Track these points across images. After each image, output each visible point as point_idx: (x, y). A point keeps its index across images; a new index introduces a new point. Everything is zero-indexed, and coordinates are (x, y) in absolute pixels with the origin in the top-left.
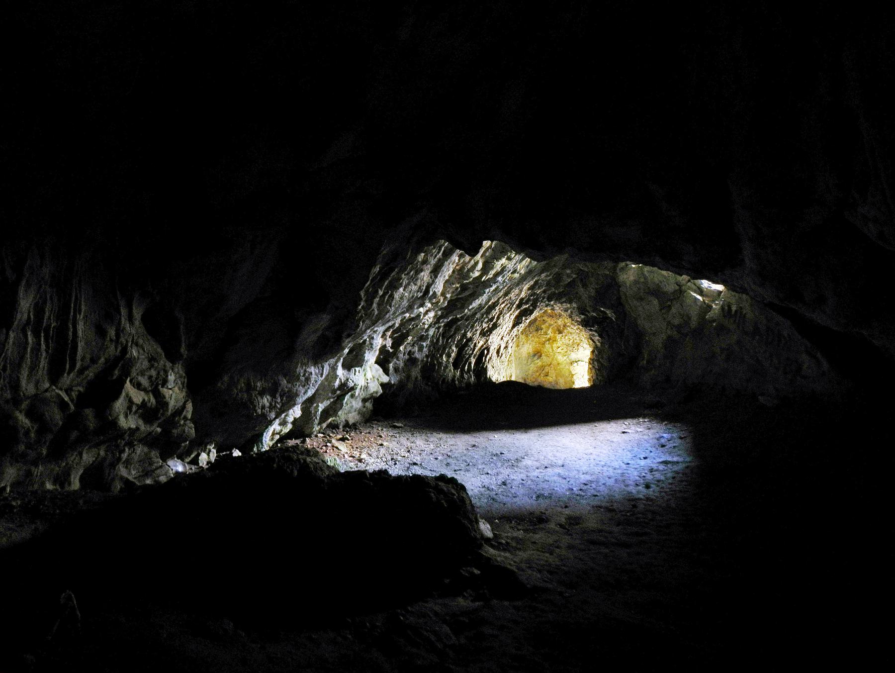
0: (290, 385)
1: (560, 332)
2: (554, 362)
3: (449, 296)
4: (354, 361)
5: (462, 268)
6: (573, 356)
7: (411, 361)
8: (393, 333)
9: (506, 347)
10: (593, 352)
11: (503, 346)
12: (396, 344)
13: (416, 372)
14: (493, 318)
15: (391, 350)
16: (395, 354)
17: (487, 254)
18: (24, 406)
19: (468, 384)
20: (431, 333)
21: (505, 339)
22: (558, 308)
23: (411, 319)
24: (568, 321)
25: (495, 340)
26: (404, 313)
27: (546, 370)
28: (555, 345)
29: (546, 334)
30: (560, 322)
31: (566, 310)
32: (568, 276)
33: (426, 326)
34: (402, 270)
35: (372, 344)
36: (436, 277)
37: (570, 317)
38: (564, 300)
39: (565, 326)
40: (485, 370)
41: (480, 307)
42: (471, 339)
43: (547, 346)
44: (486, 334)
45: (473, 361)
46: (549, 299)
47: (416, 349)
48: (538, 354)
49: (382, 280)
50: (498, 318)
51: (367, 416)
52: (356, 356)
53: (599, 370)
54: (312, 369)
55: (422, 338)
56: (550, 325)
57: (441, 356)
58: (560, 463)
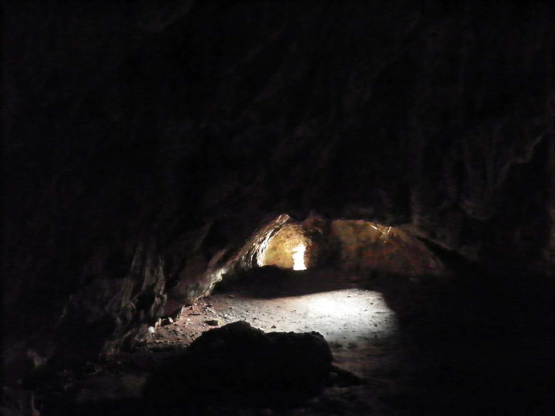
1: (288, 237)
6: (294, 250)
10: (307, 248)
18: (120, 313)
24: (294, 233)
25: (263, 245)
27: (279, 257)
28: (284, 244)
29: (280, 238)
30: (289, 233)
31: (295, 228)
37: (296, 231)
39: (291, 235)
40: (257, 260)
42: (254, 246)
43: (280, 244)
44: (260, 243)
48: (274, 249)
58: (327, 315)
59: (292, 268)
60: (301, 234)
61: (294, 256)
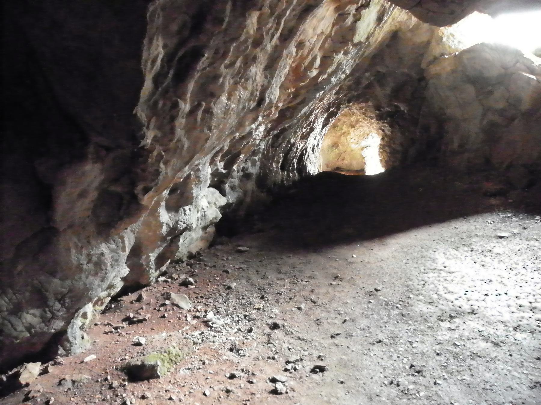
0: (68, 282)
1: (353, 127)
2: (349, 150)
3: (280, 105)
4: (180, 198)
5: (298, 67)
6: (363, 143)
7: (246, 176)
8: (223, 157)
9: (318, 145)
10: (383, 139)
11: (316, 144)
12: (228, 166)
13: (251, 185)
14: (310, 122)
15: (224, 172)
16: (228, 175)
17: (327, 45)
19: (294, 182)
20: (262, 146)
21: (317, 139)
22: (355, 108)
23: (242, 138)
24: (361, 118)
25: (311, 141)
26: (232, 133)
27: (343, 156)
28: (349, 137)
29: (341, 129)
30: (353, 119)
31: (361, 109)
32: (368, 79)
33: (258, 142)
34: (220, 55)
35: (198, 177)
36: (272, 77)
37: (364, 114)
38: (361, 100)
39: (357, 121)
40: (305, 167)
41: (305, 113)
42: (294, 144)
43: (343, 138)
44: (305, 137)
45: (295, 161)
46: (349, 102)
47: (249, 164)
48: (335, 145)
49: (181, 78)
50: (314, 122)
51: (211, 239)
52: (182, 194)
53: (390, 153)
54: (104, 248)
55: (254, 153)
56: (344, 122)
57: (272, 164)
59: (363, 170)
60: (371, 118)
61: (365, 153)
